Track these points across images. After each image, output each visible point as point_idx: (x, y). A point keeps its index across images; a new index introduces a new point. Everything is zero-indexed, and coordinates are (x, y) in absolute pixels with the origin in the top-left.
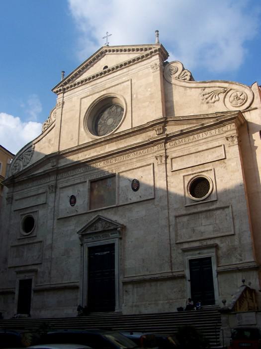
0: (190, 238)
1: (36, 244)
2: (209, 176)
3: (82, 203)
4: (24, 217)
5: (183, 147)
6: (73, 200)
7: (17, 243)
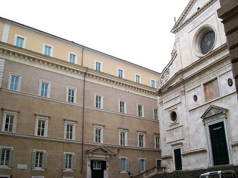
1: (179, 128)
3: (201, 99)
6: (195, 98)
7: (169, 129)
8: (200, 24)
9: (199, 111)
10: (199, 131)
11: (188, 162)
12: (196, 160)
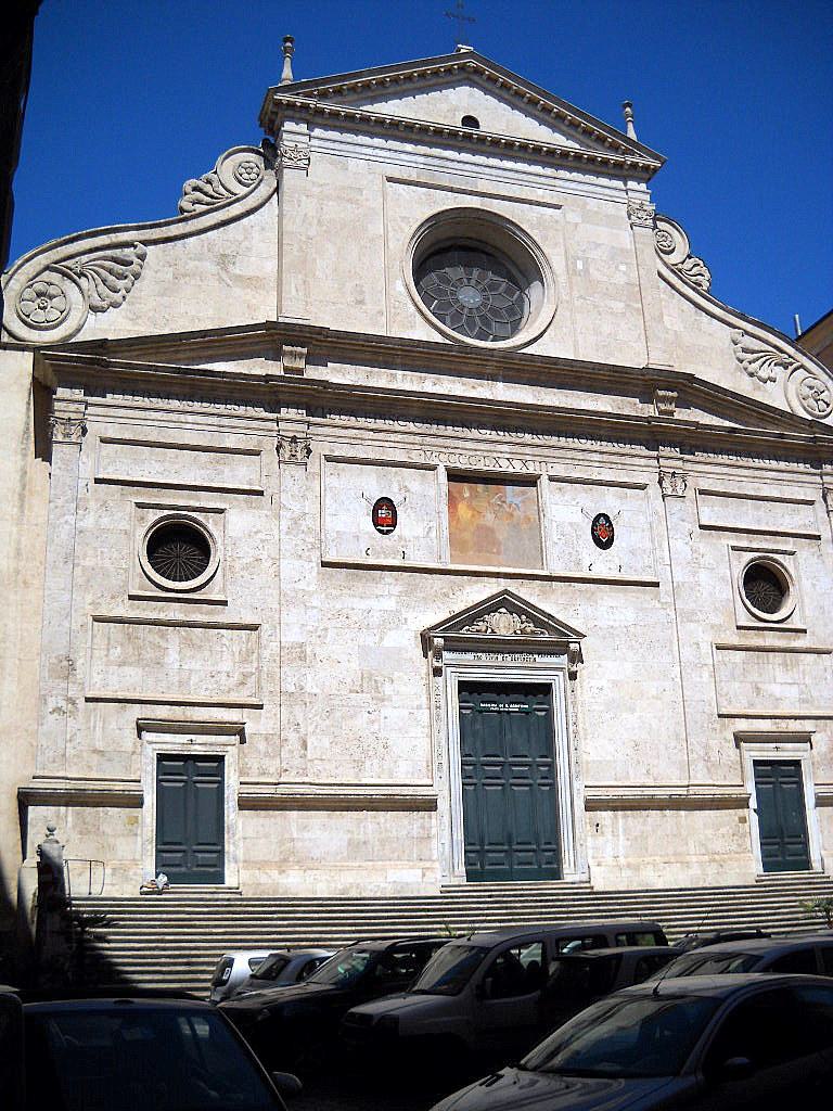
0: (749, 708)
4: (153, 516)
5: (726, 470)
8: (471, 193)
10: (388, 689)
11: (281, 843)
12: (350, 843)
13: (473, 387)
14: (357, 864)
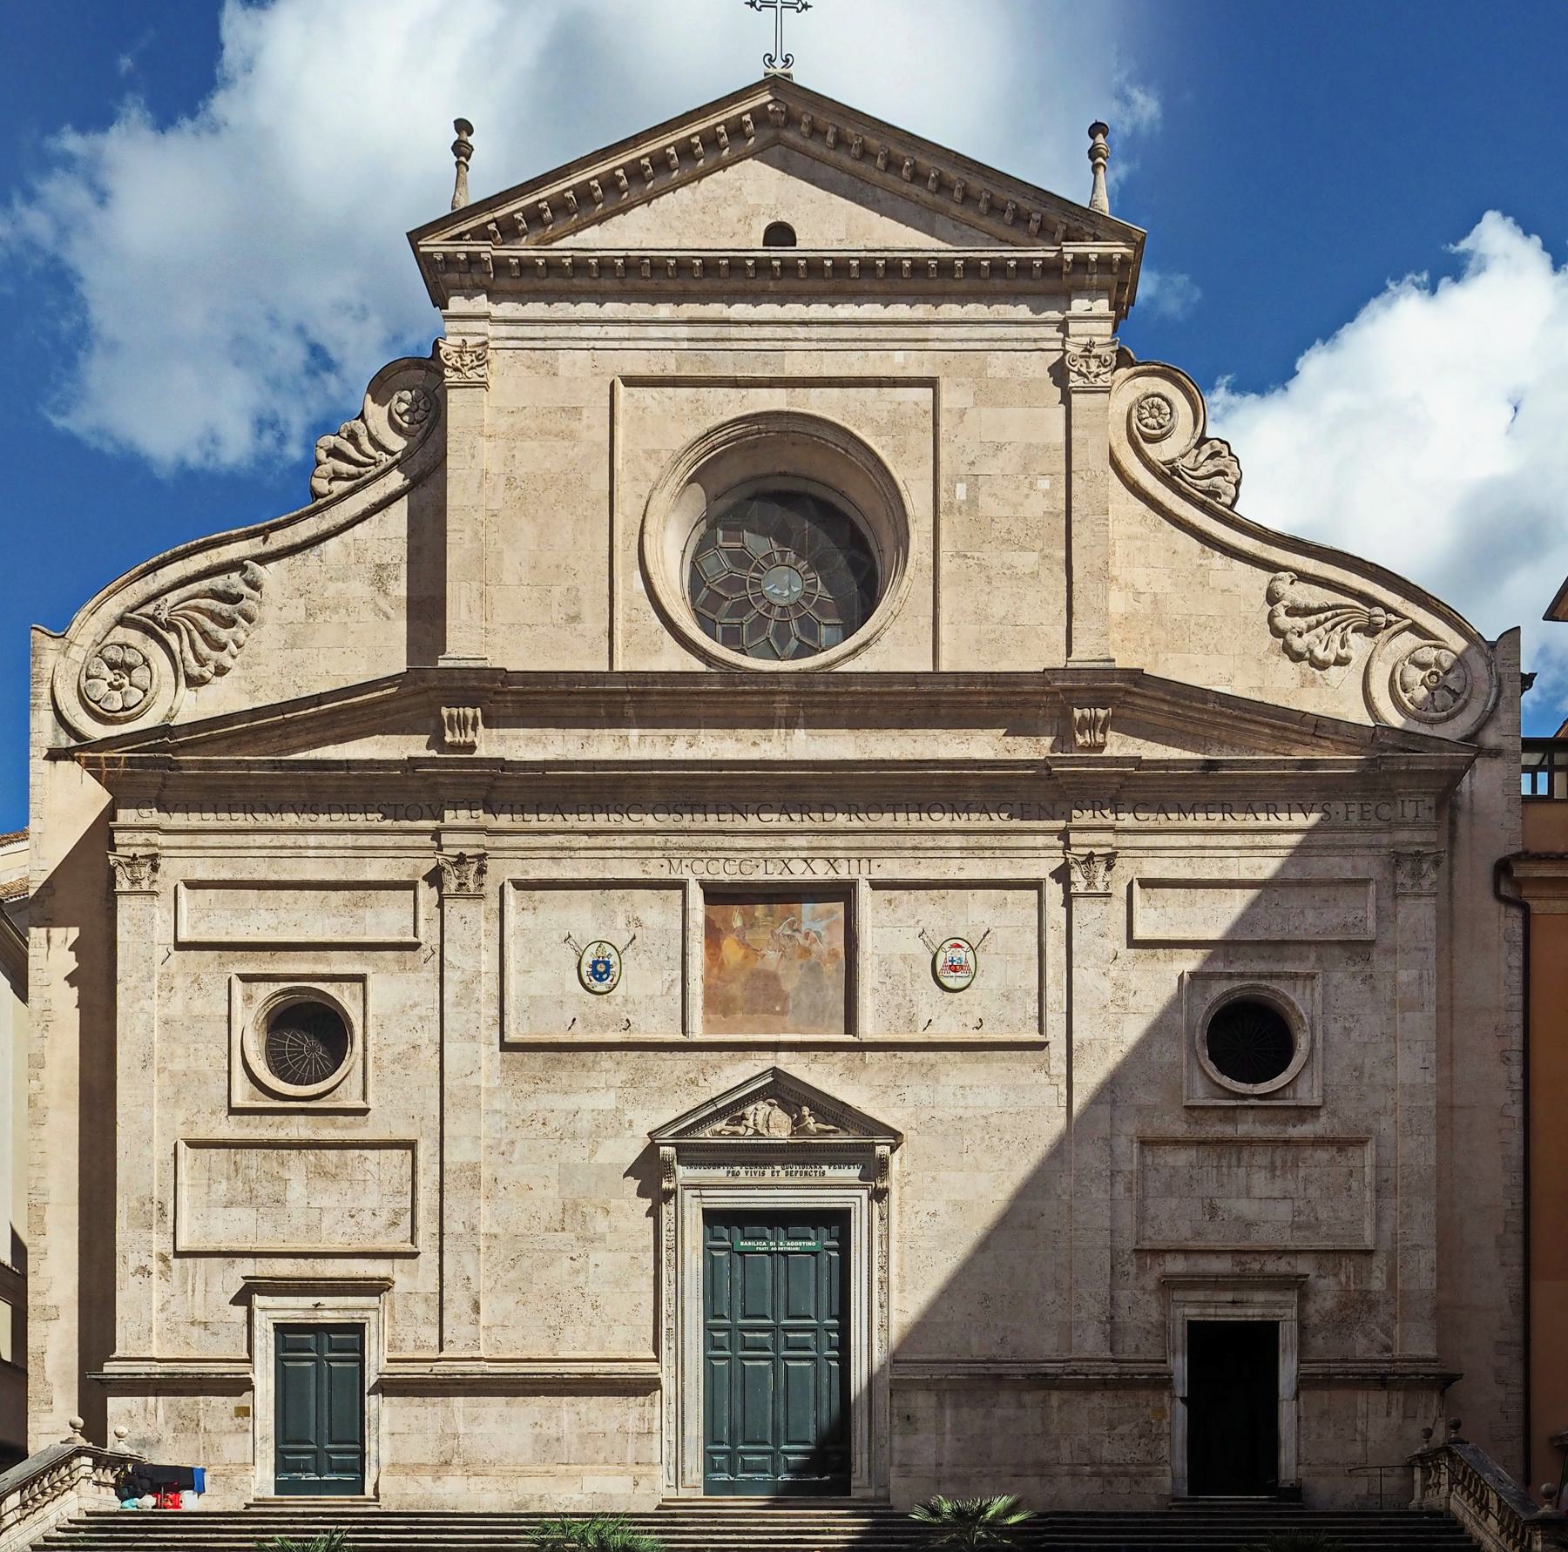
1: (366, 1153)
2: (1301, 1001)
4: (264, 991)
5: (1196, 840)
9: (623, 1076)
10: (600, 1224)
11: (442, 1438)
12: (537, 1438)
13: (754, 744)
14: (544, 1469)
